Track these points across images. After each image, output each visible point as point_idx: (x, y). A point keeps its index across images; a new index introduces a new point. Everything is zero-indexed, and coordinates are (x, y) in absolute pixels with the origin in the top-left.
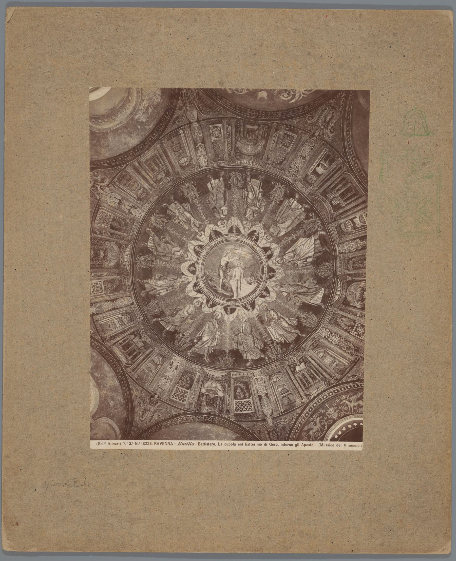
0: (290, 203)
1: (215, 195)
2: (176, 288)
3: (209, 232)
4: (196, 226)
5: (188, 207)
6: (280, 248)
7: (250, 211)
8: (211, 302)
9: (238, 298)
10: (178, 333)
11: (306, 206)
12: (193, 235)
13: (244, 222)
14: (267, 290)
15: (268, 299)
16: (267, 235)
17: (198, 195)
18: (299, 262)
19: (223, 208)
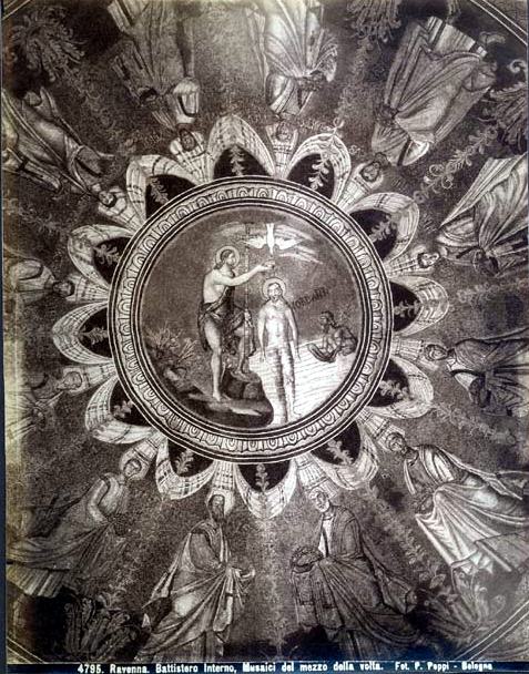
0: (430, 34)
1: (144, 45)
2: (44, 421)
3: (143, 185)
4: (89, 171)
5: (45, 100)
6: (421, 206)
7: (284, 86)
8: (189, 451)
9: (291, 420)
10: (72, 601)
11: (491, 40)
12: (82, 206)
13: (270, 130)
14: (395, 374)
15: (406, 409)
16: (361, 166)
17: (79, 55)
18: (497, 252)
19: (184, 88)
